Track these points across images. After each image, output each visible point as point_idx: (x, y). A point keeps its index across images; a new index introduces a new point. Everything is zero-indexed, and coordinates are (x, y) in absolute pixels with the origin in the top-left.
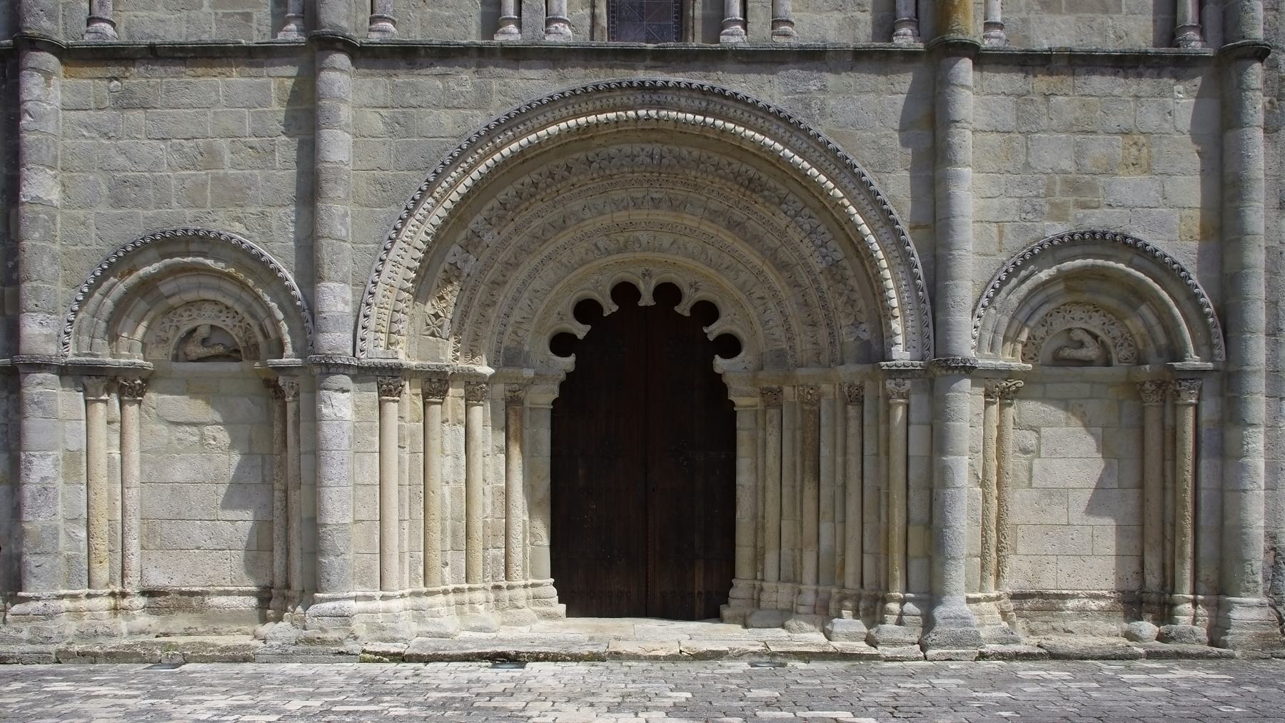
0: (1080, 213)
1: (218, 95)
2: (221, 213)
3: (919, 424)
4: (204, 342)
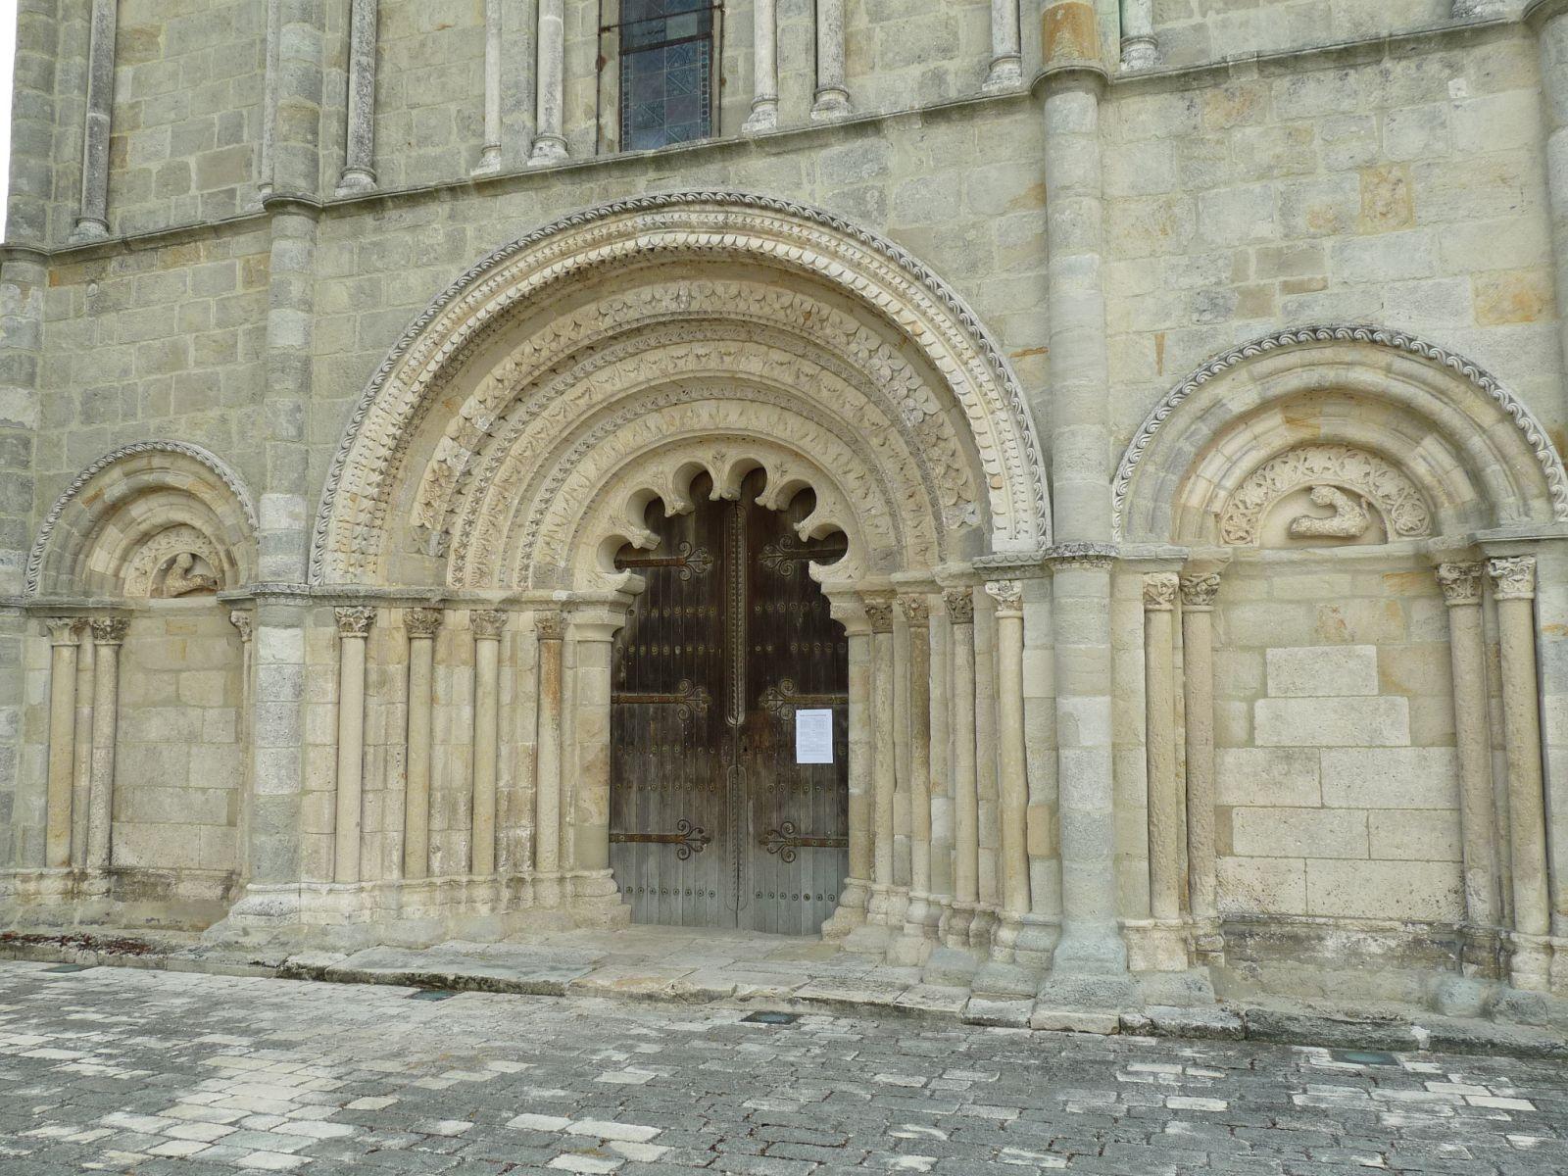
0: (1292, 299)
1: (185, 285)
2: (184, 419)
3: (1037, 647)
4: (187, 571)
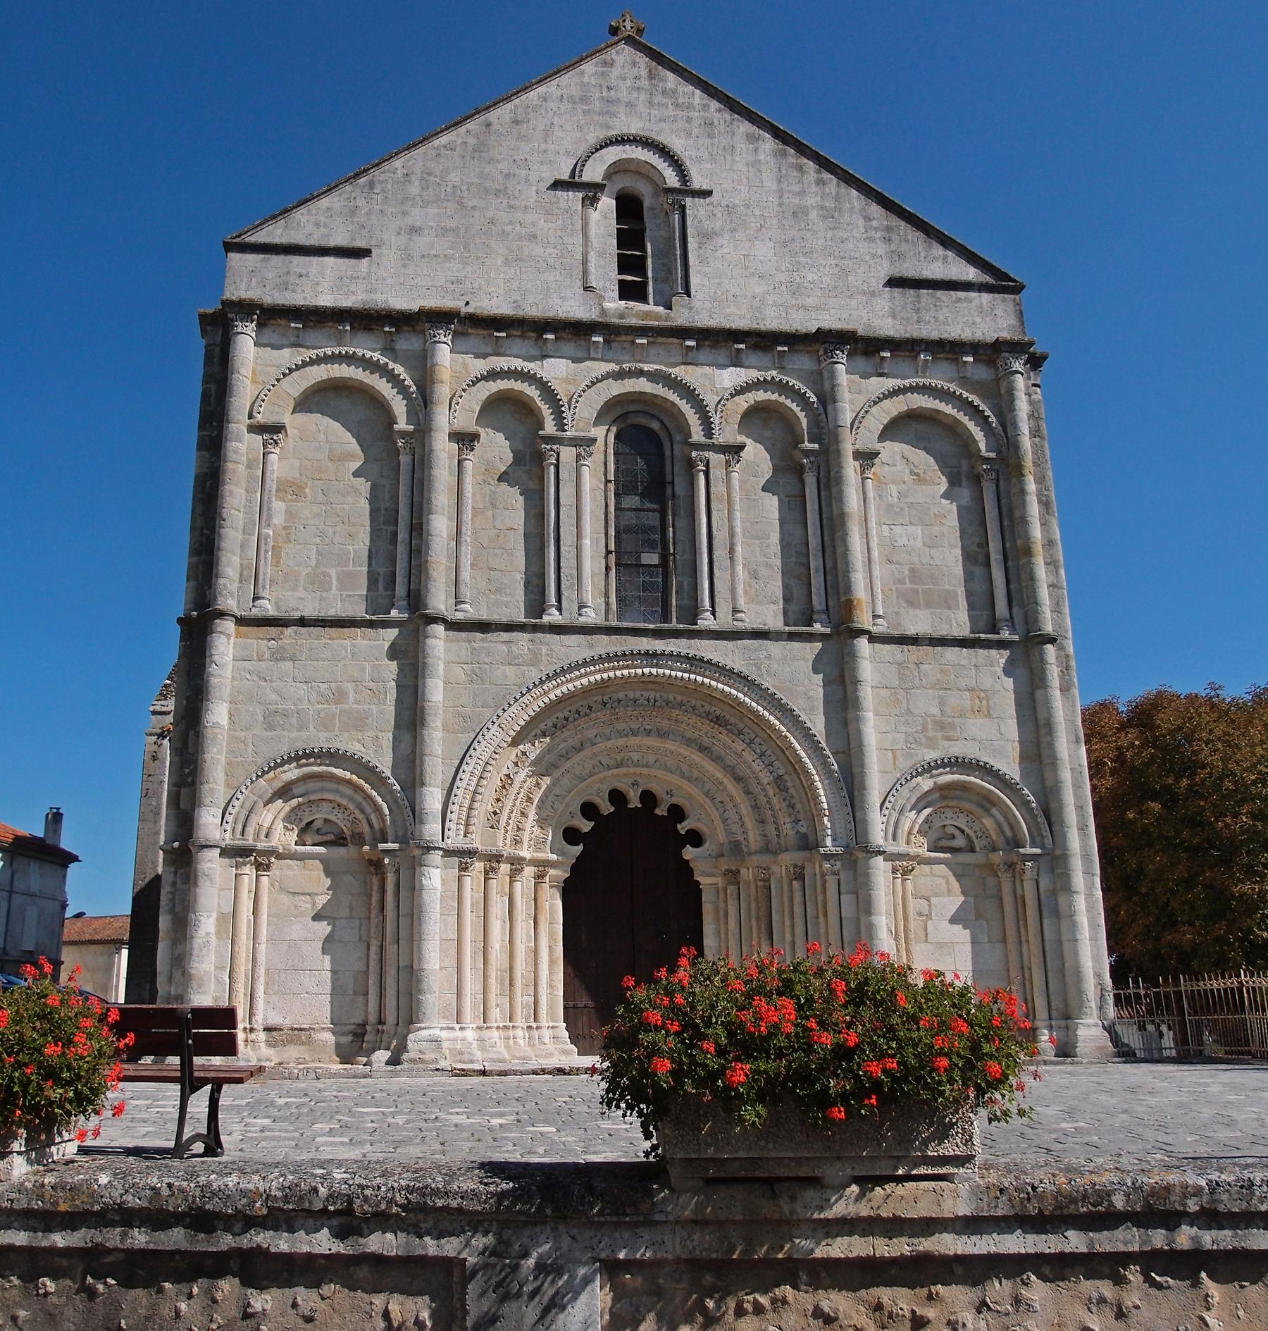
0: (947, 744)
